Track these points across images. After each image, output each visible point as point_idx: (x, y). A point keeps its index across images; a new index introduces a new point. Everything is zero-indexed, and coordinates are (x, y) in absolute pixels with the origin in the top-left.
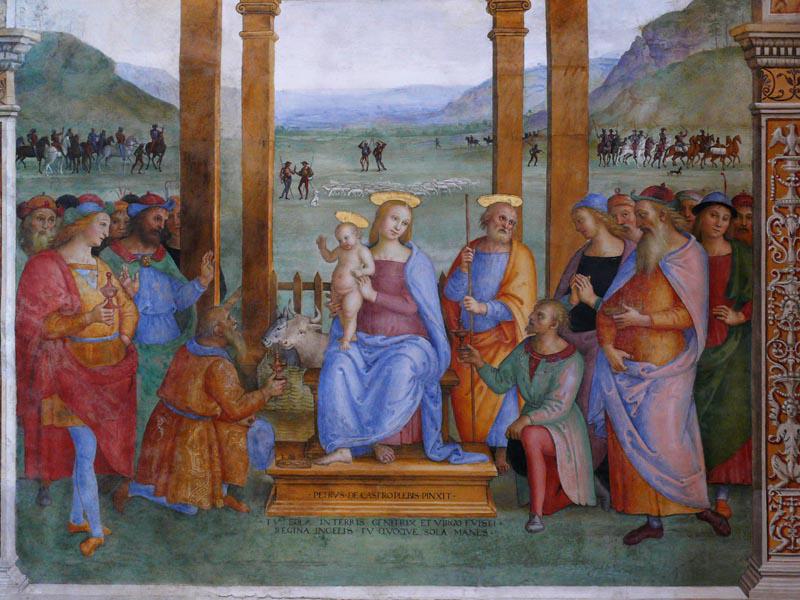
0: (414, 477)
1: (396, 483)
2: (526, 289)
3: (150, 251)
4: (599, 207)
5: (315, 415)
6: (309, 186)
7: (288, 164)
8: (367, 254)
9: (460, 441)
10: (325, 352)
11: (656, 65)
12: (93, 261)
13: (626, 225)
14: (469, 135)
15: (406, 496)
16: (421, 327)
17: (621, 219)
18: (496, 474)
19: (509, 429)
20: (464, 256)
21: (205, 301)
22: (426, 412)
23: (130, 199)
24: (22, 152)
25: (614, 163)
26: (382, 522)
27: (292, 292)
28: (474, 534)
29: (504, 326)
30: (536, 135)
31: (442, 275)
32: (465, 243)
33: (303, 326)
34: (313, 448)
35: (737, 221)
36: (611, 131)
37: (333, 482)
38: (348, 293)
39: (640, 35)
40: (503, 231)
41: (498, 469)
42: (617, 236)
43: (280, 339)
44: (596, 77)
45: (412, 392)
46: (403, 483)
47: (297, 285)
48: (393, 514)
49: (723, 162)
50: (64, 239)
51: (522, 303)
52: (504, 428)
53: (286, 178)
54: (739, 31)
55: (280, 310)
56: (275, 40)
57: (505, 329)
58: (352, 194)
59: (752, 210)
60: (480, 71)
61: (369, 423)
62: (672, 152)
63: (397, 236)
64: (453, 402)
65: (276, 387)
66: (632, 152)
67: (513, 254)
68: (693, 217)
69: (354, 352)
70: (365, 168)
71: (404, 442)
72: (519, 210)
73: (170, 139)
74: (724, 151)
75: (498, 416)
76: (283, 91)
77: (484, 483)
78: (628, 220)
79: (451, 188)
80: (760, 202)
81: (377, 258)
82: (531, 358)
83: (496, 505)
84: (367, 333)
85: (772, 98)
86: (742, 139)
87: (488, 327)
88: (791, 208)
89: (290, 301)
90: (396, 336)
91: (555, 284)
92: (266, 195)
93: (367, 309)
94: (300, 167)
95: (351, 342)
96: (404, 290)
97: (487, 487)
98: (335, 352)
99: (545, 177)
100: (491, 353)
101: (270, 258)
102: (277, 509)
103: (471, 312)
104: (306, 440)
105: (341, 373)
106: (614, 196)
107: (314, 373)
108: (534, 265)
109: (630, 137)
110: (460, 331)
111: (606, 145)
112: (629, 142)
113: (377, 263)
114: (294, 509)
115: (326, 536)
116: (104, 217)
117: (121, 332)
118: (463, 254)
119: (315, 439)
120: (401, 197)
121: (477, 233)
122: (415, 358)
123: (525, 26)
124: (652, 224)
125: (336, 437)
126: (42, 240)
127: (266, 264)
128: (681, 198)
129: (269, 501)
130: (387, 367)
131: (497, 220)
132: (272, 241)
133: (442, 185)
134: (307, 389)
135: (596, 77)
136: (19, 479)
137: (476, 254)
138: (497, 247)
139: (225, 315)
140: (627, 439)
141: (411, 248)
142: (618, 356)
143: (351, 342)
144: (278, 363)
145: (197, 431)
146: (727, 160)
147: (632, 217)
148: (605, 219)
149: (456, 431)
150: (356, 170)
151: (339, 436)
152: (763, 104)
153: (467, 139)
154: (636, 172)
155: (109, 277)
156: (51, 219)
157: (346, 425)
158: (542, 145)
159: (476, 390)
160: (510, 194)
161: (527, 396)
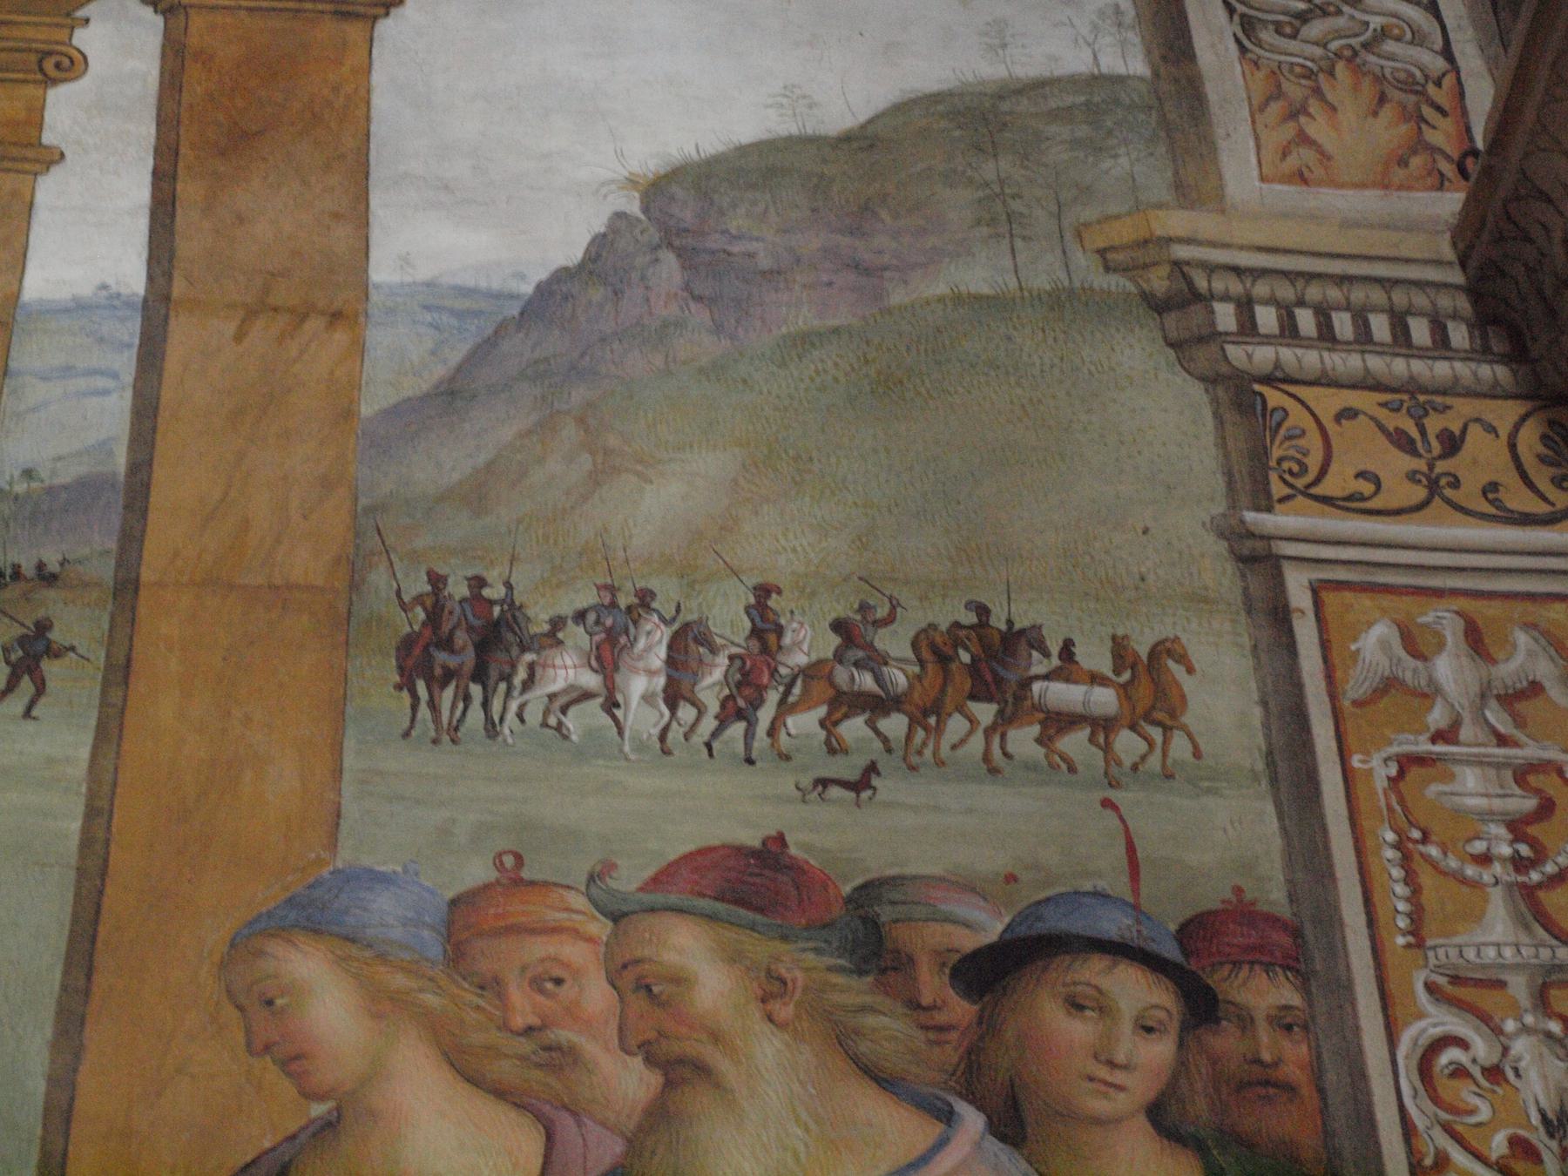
4: (397, 933)
11: (718, 329)
13: (564, 1035)
17: (523, 1006)
25: (492, 728)
30: (47, 578)
35: (1225, 1041)
36: (478, 582)
39: (634, 208)
42: (500, 1093)
49: (1107, 748)
54: (1124, 232)
59: (1305, 990)
62: (820, 689)
66: (591, 680)
68: (961, 1010)
74: (1104, 699)
78: (572, 1012)
80: (1336, 950)
85: (1326, 500)
86: (1198, 651)
88: (1519, 987)
106: (487, 887)
109: (580, 616)
111: (447, 644)
112: (576, 636)
123: (48, 138)
124: (716, 1037)
128: (885, 913)
146: (1127, 743)
147: (597, 995)
148: (431, 999)
152: (1281, 521)
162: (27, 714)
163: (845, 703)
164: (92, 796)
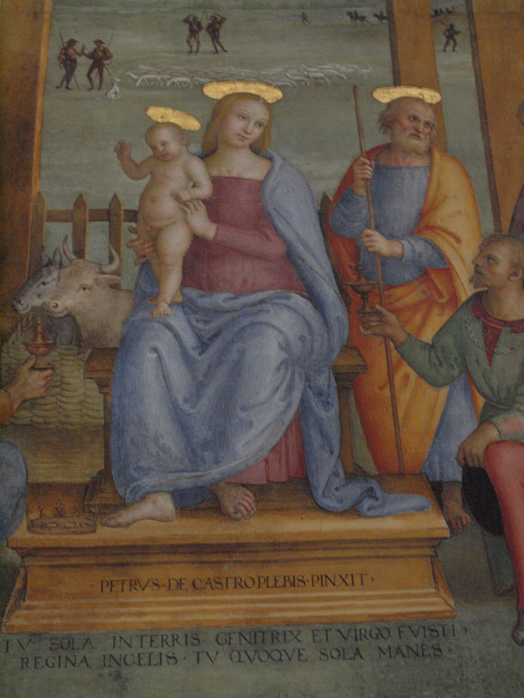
1: (261, 557)
6: (105, 72)
7: (72, 43)
9: (375, 472)
10: (124, 323)
14: (352, 10)
15: (281, 582)
18: (447, 534)
19: (462, 449)
20: (357, 170)
22: (311, 421)
26: (235, 638)
27: (69, 226)
28: (417, 654)
29: (433, 276)
30: (450, 12)
31: (325, 198)
32: (356, 150)
37: (138, 559)
38: (167, 226)
40: (416, 135)
41: (449, 523)
43: (46, 299)
45: (284, 387)
46: (267, 556)
48: (257, 621)
51: (458, 240)
55: (49, 252)
57: (437, 282)
58: (173, 84)
61: (206, 445)
63: (247, 142)
64: (356, 398)
67: (436, 169)
70: (194, 48)
71: (272, 479)
72: (437, 108)
75: (439, 427)
77: (428, 552)
79: (330, 77)
81: (215, 173)
82: (485, 327)
83: (452, 591)
84: (201, 289)
87: (407, 277)
89: (66, 238)
90: (253, 291)
91: (507, 211)
92: (35, 83)
94: (90, 47)
95: (172, 305)
97: (433, 559)
98: (147, 320)
99: (470, 65)
100: (418, 319)
101: (35, 173)
102: (27, 618)
103: (377, 254)
104: (88, 479)
105: (155, 355)
108: (471, 185)
114: (61, 616)
115: (125, 671)
118: (354, 167)
120: (252, 89)
122: (285, 330)
125: (146, 472)
127: (28, 180)
129: (11, 602)
130: (238, 346)
131: (406, 122)
132: (40, 149)
133: (315, 72)
134: (93, 386)
137: (378, 169)
138: (408, 159)
141: (271, 159)
143: (172, 305)
144: (40, 341)
149: (368, 455)
150: (181, 52)
151: (150, 469)
153: (349, 14)
157: (164, 449)
158: (461, 25)
159: (398, 380)
160: (420, 87)
161: (487, 390)
162: (454, 50)
164: (475, 72)
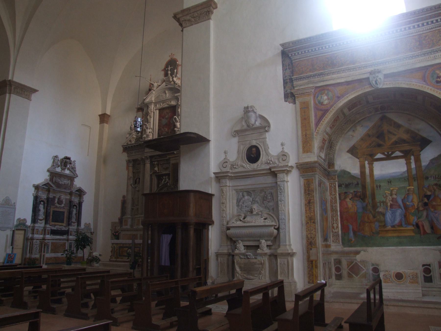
0: (401, 230)
2: (416, 200)
3: (358, 199)
5: (385, 221)
7: (377, 185)
8: (390, 197)
12: (350, 201)
16: (400, 207)
21: (367, 205)
23: (354, 192)
24: (339, 186)
33: (382, 208)
34: (385, 226)
44: (423, 168)
47: (380, 202)
50: (345, 198)
51: (415, 203)
52: (415, 222)
53: (377, 187)
56: (373, 167)
60: (405, 169)
65: (378, 217)
69: (390, 211)
72: (413, 189)
73: (359, 183)
76: (376, 175)
93: (391, 205)
94: (379, 185)
95: (389, 210)
96: (397, 202)
107: (384, 215)
110: (406, 207)
113: (392, 198)
116: (351, 194)
117: (354, 211)
119: (385, 225)
120: (395, 188)
121: (407, 192)
126: (342, 198)
135: (423, 168)
136: (342, 232)
139: (370, 207)
140: (435, 222)
141: (397, 196)
142: (432, 210)
143: (389, 210)
145: (367, 224)
154: (432, 181)
155: (352, 203)
156: (343, 195)
158: (416, 179)
163: (438, 178)
